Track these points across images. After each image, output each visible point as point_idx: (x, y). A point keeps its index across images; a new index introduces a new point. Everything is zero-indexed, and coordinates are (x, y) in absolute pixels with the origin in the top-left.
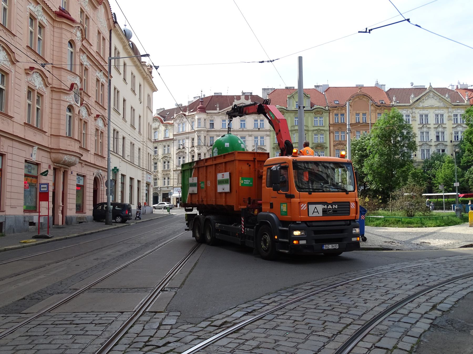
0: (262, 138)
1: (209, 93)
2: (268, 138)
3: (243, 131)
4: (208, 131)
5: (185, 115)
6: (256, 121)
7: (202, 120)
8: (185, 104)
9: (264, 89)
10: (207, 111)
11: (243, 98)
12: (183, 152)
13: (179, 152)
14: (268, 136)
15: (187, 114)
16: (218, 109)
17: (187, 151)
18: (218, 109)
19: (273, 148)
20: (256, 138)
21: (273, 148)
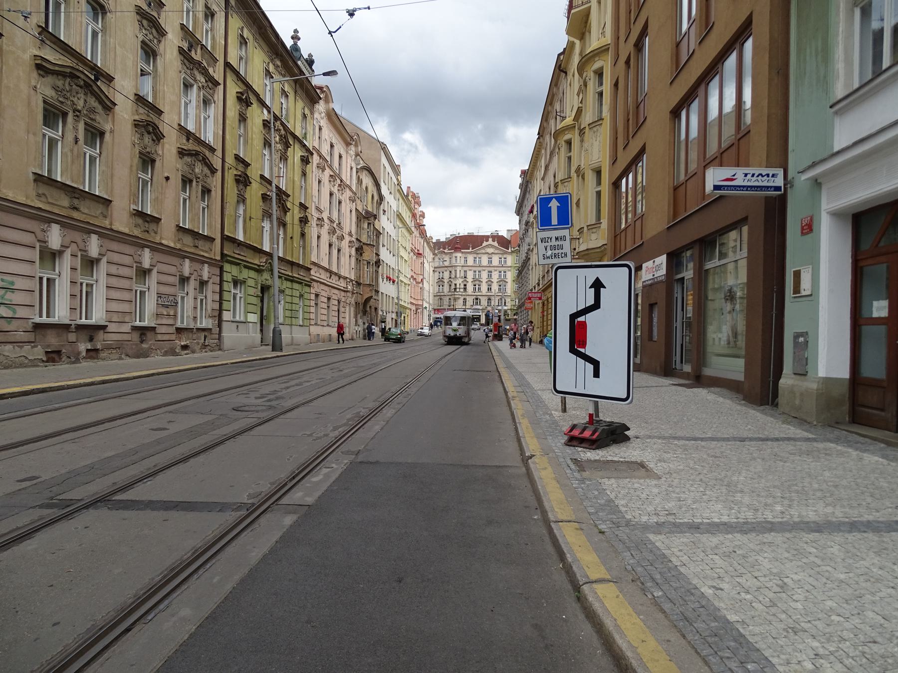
0: (505, 272)
1: (463, 232)
2: (510, 272)
3: (490, 266)
4: (463, 266)
5: (444, 252)
6: (500, 258)
7: (458, 258)
8: (443, 239)
9: (508, 230)
10: (462, 251)
11: (490, 239)
12: (443, 281)
13: (438, 282)
14: (509, 271)
15: (446, 251)
16: (471, 248)
17: (446, 281)
18: (471, 248)
19: (514, 281)
20: (500, 272)
21: (514, 281)
